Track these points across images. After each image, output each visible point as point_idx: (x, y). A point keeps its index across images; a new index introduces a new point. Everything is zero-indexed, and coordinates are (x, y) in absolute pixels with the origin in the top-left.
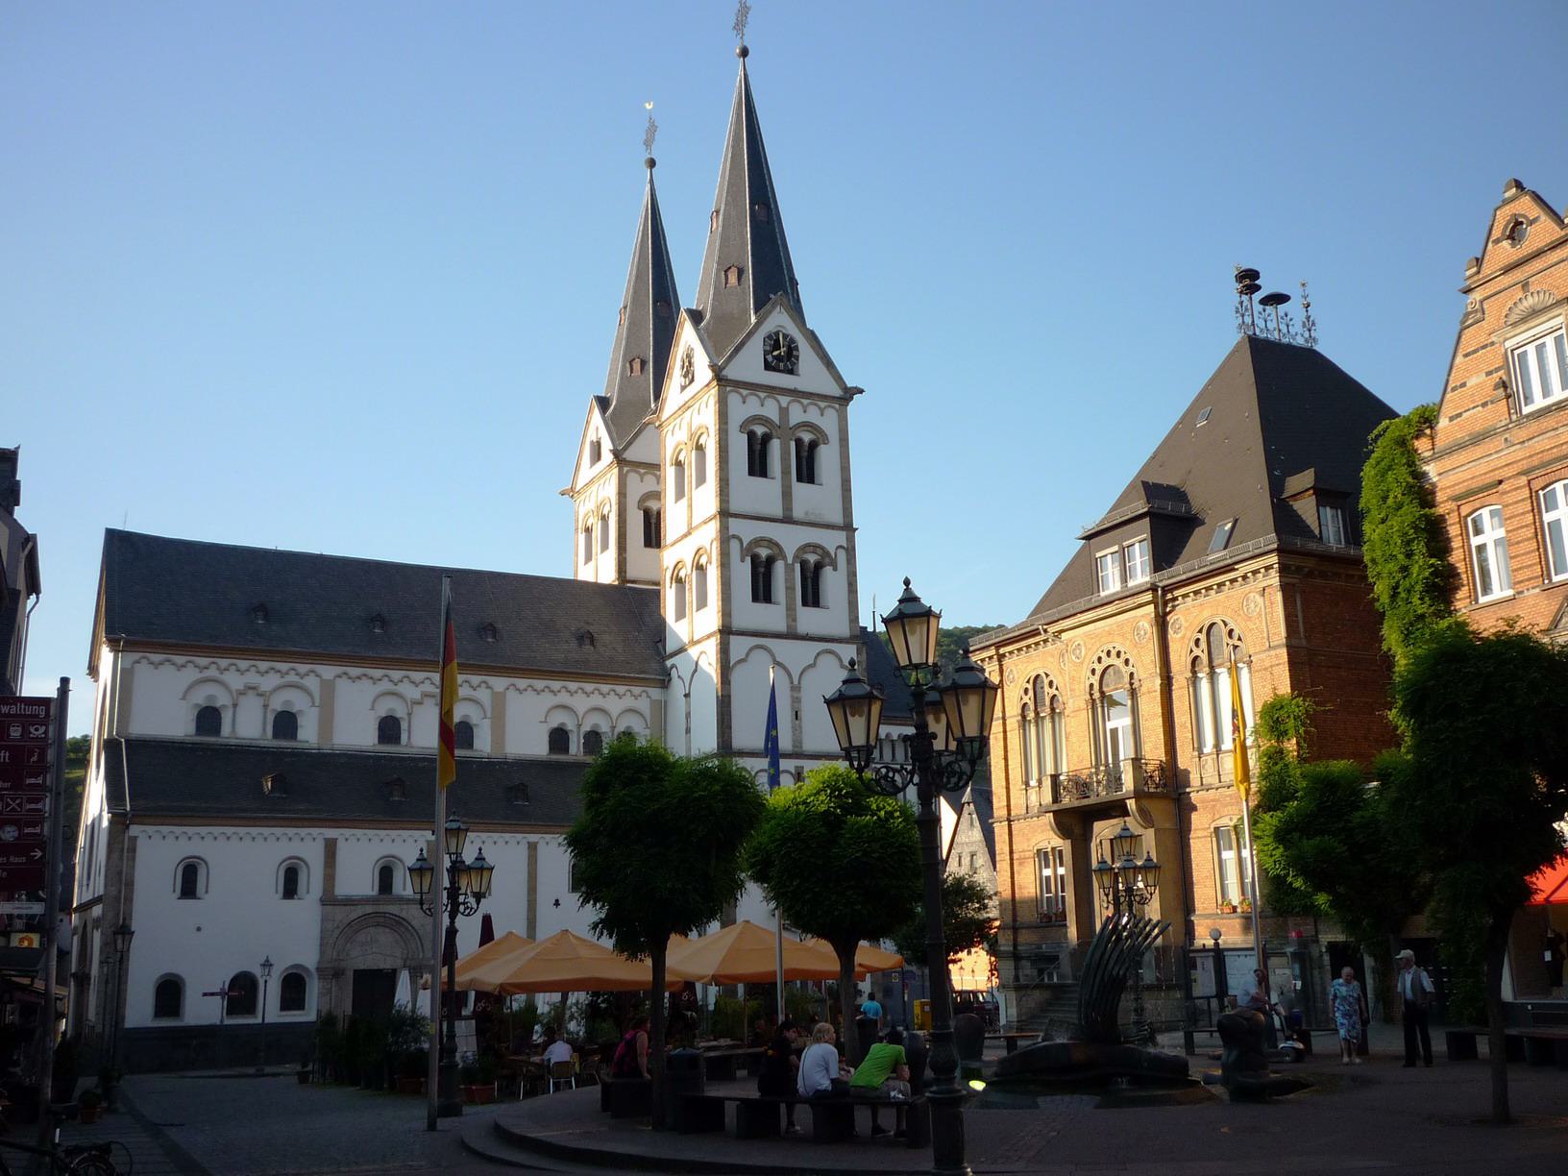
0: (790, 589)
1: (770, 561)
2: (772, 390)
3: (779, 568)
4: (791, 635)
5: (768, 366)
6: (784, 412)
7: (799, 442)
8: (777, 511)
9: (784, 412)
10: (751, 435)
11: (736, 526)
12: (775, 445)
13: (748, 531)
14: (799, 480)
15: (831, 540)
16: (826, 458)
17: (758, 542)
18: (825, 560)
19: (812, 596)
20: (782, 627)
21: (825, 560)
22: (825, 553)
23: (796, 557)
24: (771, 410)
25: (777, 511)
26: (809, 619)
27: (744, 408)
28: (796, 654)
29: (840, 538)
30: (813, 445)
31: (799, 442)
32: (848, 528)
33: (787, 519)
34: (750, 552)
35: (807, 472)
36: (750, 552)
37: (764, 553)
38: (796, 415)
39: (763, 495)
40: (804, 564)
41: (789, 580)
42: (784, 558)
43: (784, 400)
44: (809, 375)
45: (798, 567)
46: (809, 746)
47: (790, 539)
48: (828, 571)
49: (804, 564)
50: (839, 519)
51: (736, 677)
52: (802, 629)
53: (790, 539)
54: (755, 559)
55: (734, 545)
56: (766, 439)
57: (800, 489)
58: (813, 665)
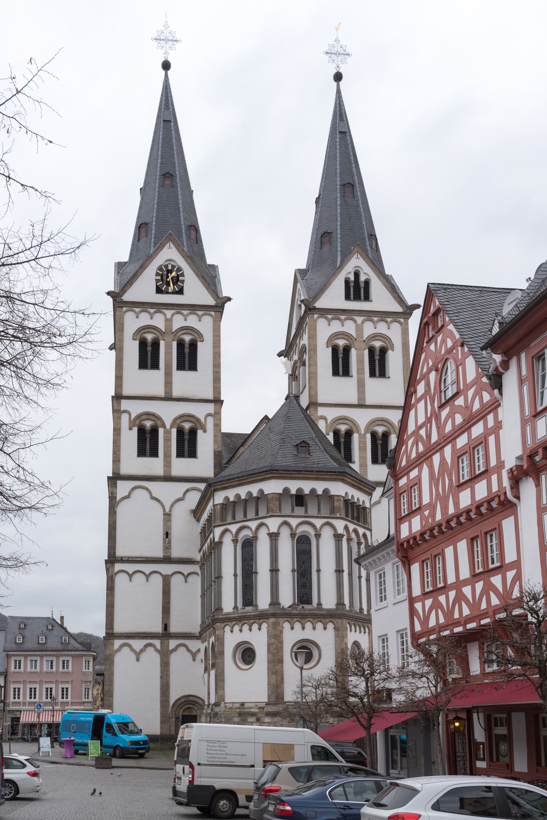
4: (168, 478)
8: (161, 392)
11: (125, 405)
14: (181, 367)
16: (204, 352)
25: (161, 392)
26: (181, 466)
27: (133, 322)
28: (168, 492)
29: (210, 408)
32: (218, 401)
33: (168, 398)
39: (152, 381)
41: (167, 440)
42: (164, 426)
46: (175, 553)
47: (168, 413)
51: (121, 509)
52: (175, 472)
53: (168, 413)
55: (125, 418)
57: (179, 376)
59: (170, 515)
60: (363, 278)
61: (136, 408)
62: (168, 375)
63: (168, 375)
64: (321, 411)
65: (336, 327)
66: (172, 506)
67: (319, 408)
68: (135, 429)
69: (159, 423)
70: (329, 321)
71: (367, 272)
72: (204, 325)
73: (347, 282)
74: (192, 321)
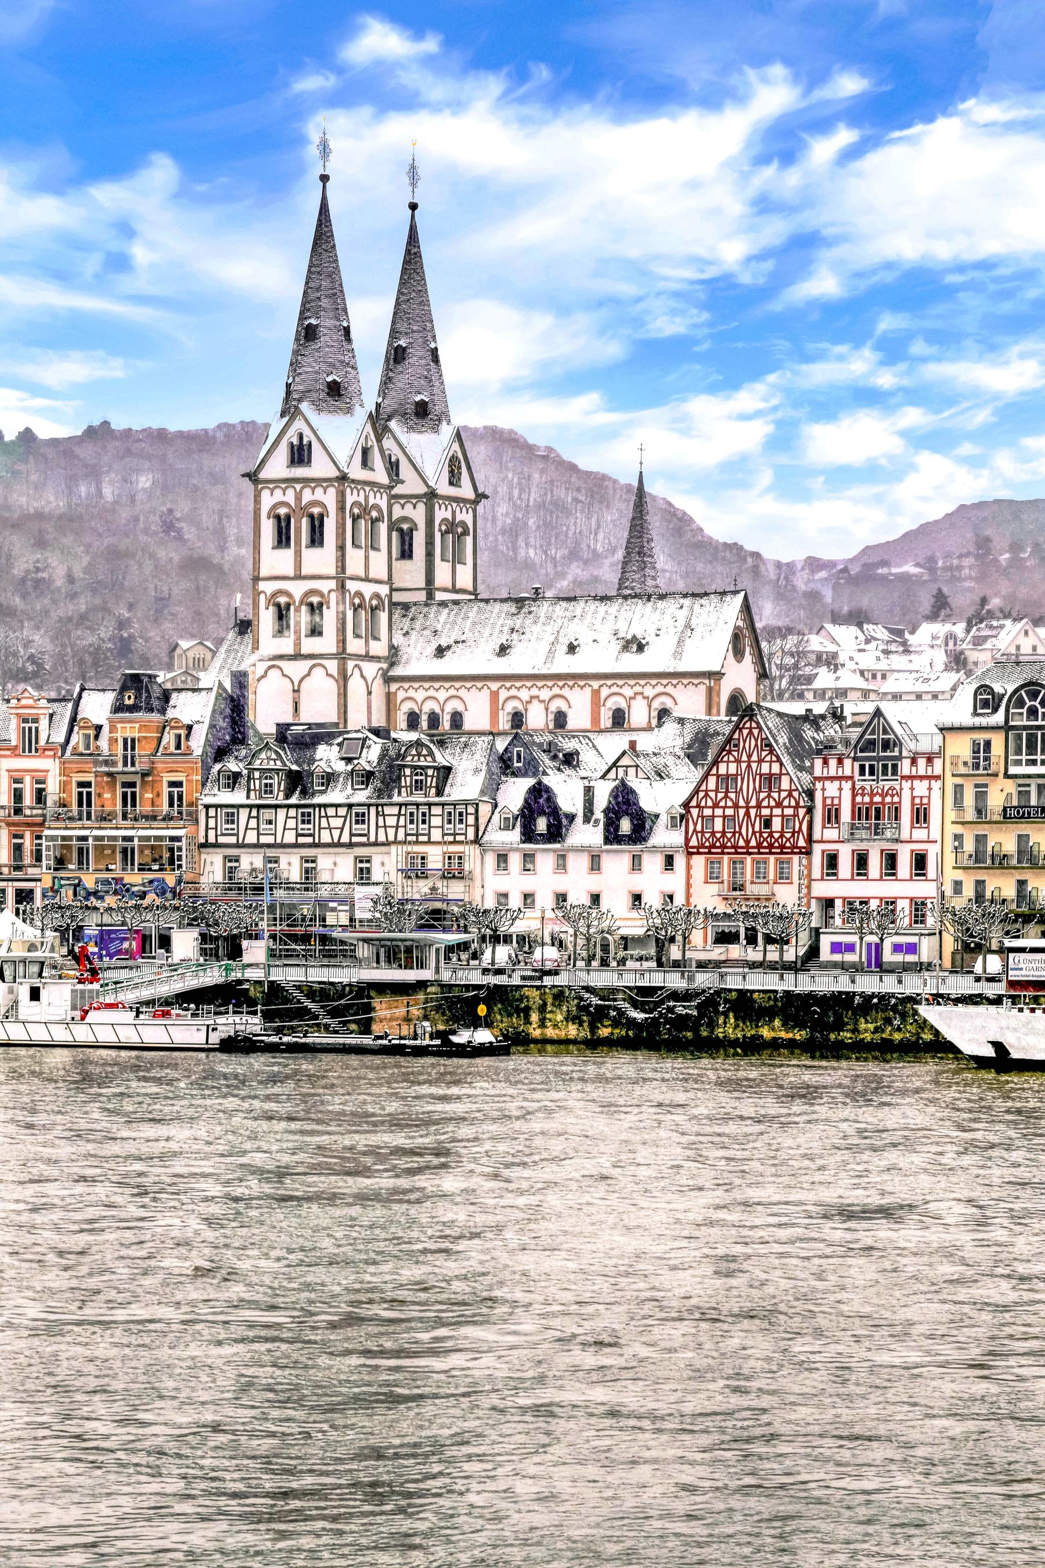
3: (292, 608)
4: (297, 656)
6: (298, 497)
7: (311, 517)
9: (298, 497)
13: (268, 587)
17: (275, 595)
20: (291, 651)
22: (322, 595)
23: (301, 603)
24: (290, 497)
26: (310, 645)
28: (296, 669)
33: (299, 577)
37: (282, 600)
53: (298, 589)
56: (288, 518)
58: (308, 674)
59: (298, 691)
62: (298, 554)
63: (298, 554)
66: (301, 682)
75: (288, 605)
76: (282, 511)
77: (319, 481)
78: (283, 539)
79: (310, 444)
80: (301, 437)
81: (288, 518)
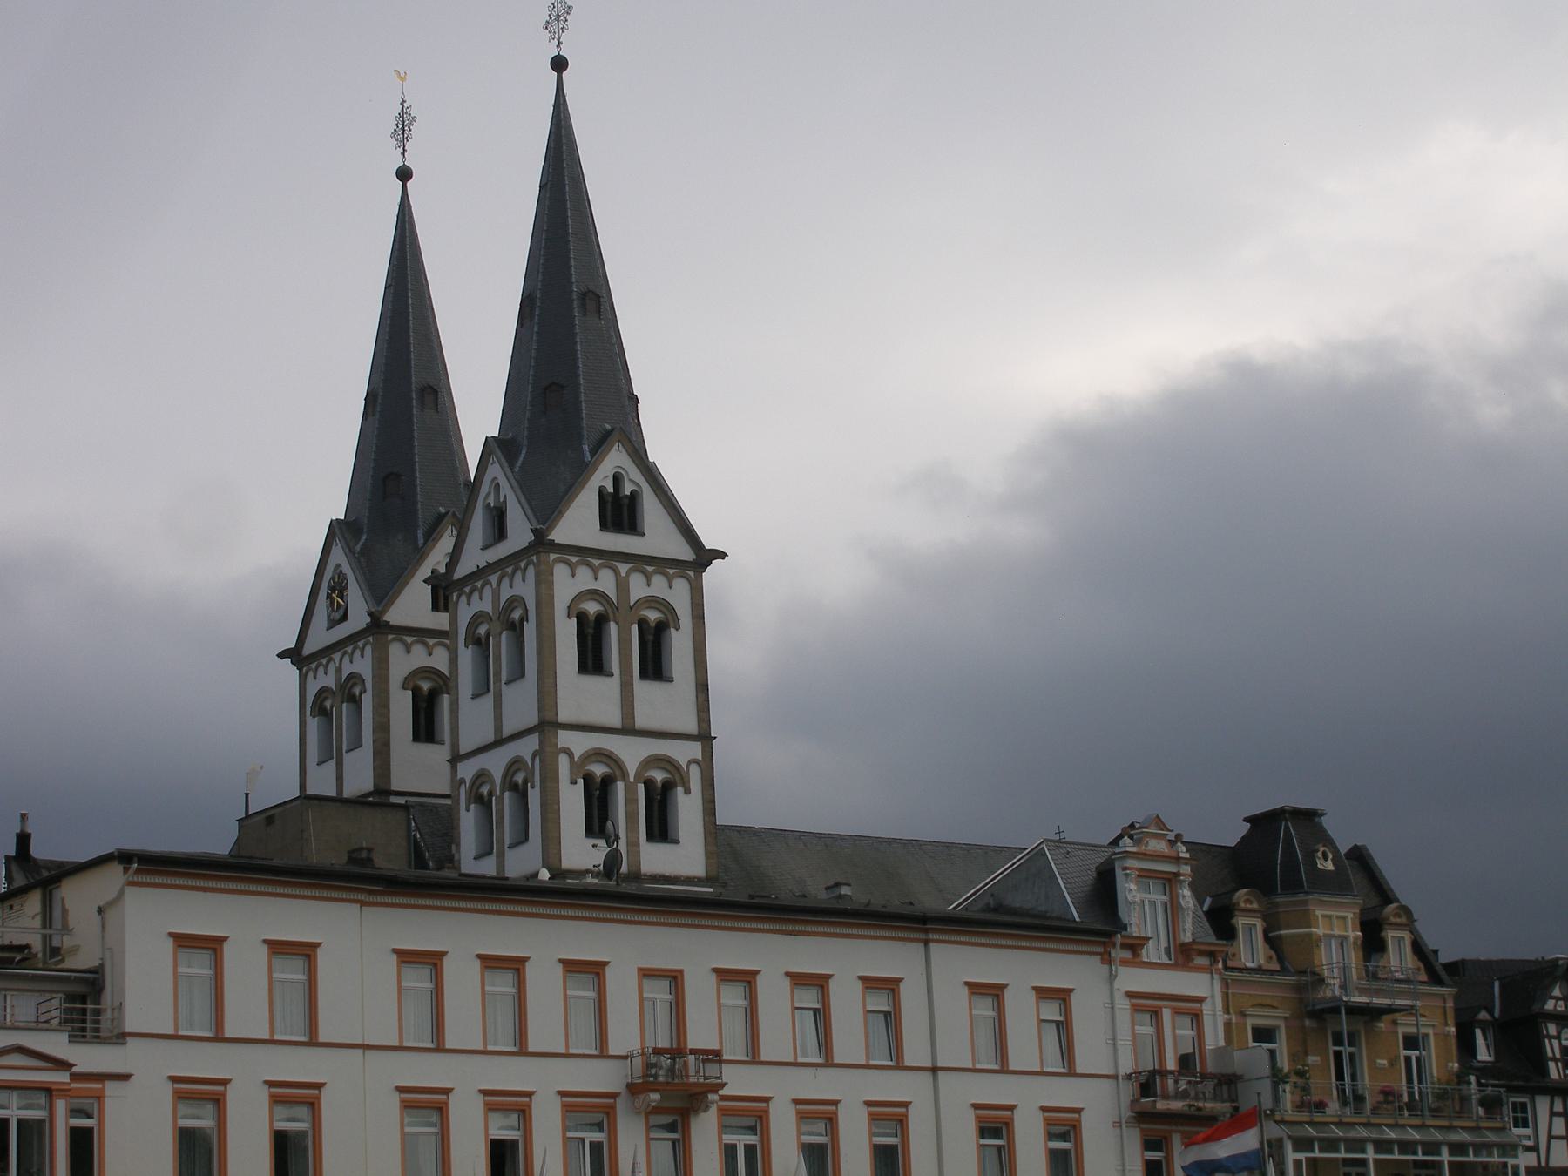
0: (631, 817)
1: (607, 782)
2: (610, 557)
3: (620, 785)
5: (604, 526)
6: (622, 586)
7: (642, 623)
10: (582, 618)
12: (613, 628)
15: (685, 753)
16: (679, 644)
18: (676, 778)
19: (661, 829)
21: (676, 778)
23: (637, 776)
24: (606, 583)
29: (695, 750)
30: (661, 628)
31: (642, 623)
33: (628, 729)
34: (579, 768)
35: (654, 666)
36: (579, 768)
37: (599, 770)
38: (638, 588)
40: (649, 784)
42: (625, 776)
43: (623, 568)
44: (657, 538)
45: (641, 787)
47: (632, 753)
48: (680, 790)
49: (649, 784)
50: (691, 726)
54: (588, 778)
56: (601, 620)
60: (628, 489)
61: (579, 743)
64: (565, 738)
65: (585, 579)
67: (560, 732)
68: (581, 781)
69: (618, 773)
70: (572, 567)
71: (634, 479)
72: (678, 595)
73: (602, 491)
74: (659, 586)
75: (607, 782)
76: (592, 608)
77: (663, 564)
78: (592, 660)
79: (634, 497)
80: (617, 479)
81: (601, 620)
